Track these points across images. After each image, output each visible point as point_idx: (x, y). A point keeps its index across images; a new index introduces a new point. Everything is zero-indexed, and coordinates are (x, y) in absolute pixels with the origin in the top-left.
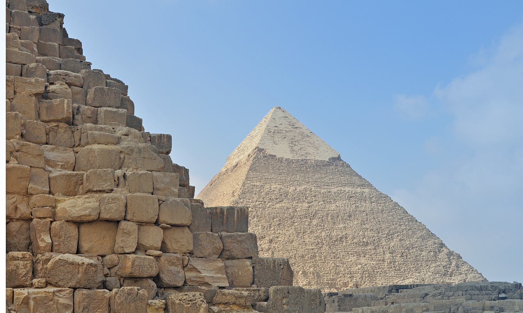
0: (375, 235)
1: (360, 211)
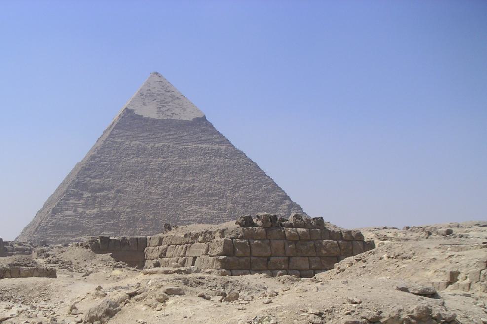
0: (222, 187)
1: (212, 166)
